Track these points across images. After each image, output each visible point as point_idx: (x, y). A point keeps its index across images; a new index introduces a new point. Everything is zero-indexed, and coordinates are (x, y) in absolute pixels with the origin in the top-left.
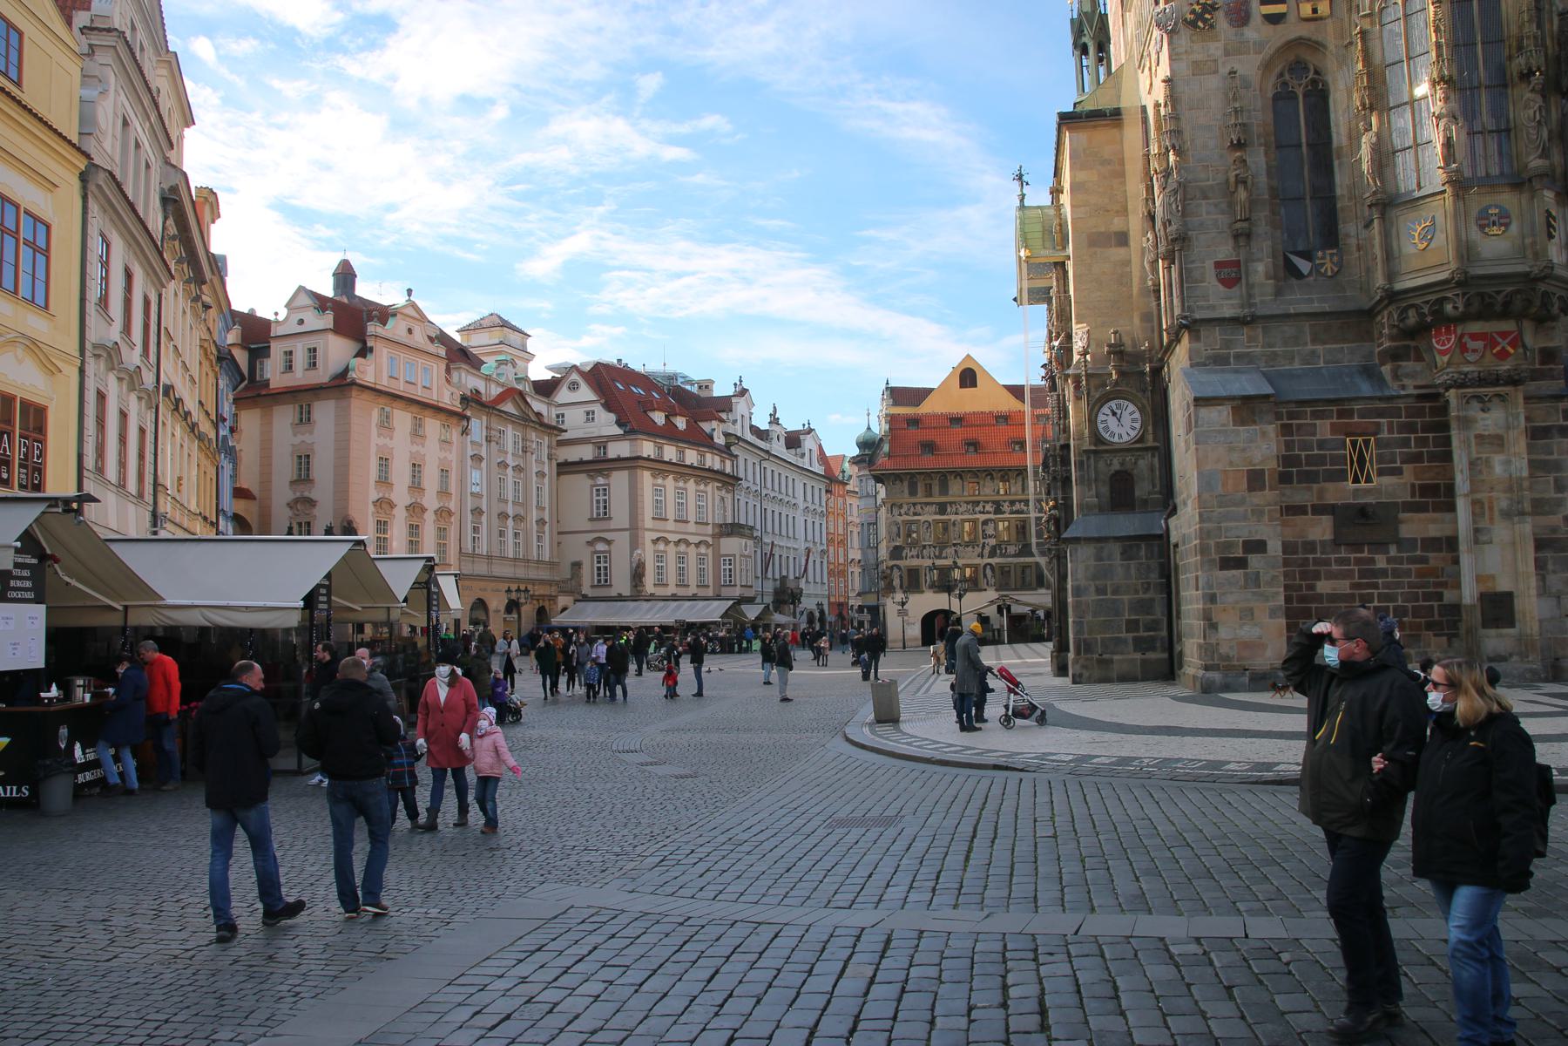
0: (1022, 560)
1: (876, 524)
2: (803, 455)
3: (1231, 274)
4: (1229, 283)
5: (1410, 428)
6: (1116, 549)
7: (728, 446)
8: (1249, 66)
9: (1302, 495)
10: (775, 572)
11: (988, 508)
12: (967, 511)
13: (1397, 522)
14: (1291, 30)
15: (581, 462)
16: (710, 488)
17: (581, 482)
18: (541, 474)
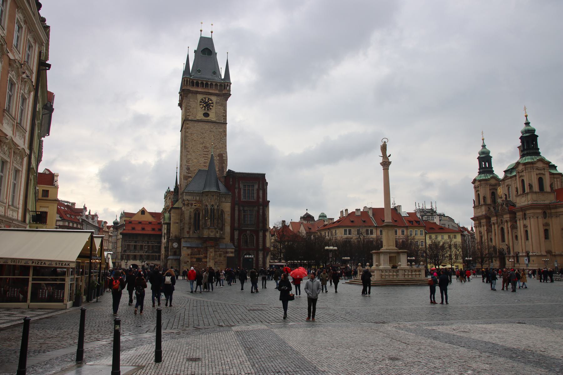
0: (152, 254)
1: (116, 242)
2: (94, 222)
3: (188, 232)
6: (174, 260)
7: (82, 222)
8: (192, 210)
9: (193, 256)
12: (141, 243)
14: (197, 207)
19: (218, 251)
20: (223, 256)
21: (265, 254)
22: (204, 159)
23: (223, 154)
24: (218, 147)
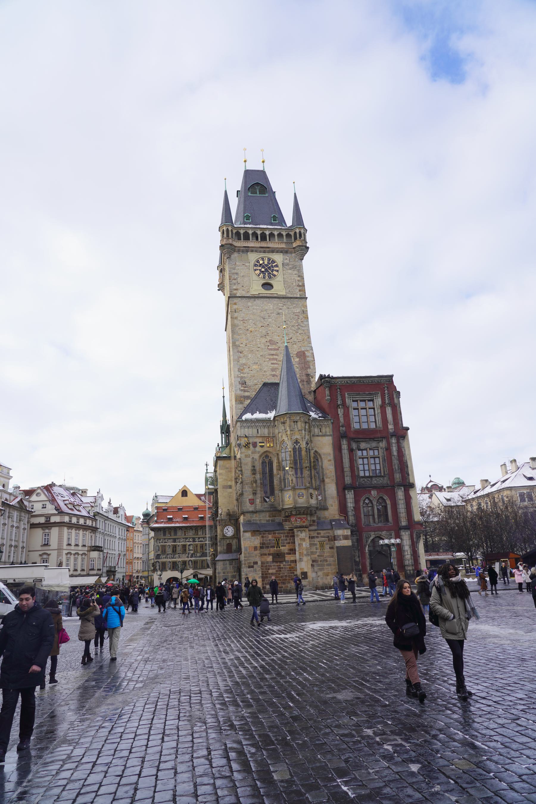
0: (202, 558)
1: (148, 545)
2: (119, 517)
3: (252, 502)
4: (252, 504)
5: (287, 536)
6: (228, 562)
7: (94, 516)
8: (256, 456)
9: (266, 551)
10: (107, 564)
11: (191, 540)
12: (183, 541)
13: (285, 557)
14: (265, 449)
15: (39, 524)
16: (88, 533)
17: (39, 533)
18: (24, 529)
19: (317, 537)
20: (327, 547)
21: (415, 536)
22: (272, 364)
23: (306, 352)
24: (296, 340)
